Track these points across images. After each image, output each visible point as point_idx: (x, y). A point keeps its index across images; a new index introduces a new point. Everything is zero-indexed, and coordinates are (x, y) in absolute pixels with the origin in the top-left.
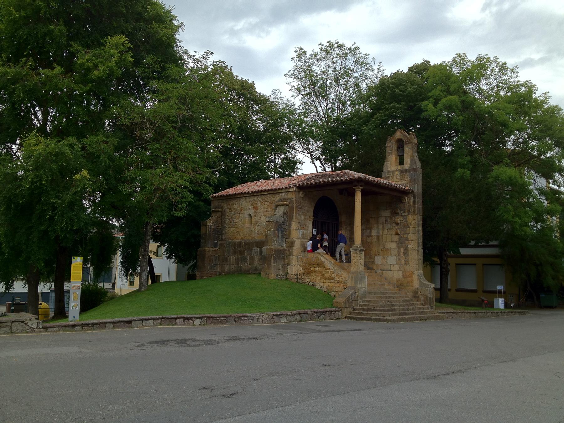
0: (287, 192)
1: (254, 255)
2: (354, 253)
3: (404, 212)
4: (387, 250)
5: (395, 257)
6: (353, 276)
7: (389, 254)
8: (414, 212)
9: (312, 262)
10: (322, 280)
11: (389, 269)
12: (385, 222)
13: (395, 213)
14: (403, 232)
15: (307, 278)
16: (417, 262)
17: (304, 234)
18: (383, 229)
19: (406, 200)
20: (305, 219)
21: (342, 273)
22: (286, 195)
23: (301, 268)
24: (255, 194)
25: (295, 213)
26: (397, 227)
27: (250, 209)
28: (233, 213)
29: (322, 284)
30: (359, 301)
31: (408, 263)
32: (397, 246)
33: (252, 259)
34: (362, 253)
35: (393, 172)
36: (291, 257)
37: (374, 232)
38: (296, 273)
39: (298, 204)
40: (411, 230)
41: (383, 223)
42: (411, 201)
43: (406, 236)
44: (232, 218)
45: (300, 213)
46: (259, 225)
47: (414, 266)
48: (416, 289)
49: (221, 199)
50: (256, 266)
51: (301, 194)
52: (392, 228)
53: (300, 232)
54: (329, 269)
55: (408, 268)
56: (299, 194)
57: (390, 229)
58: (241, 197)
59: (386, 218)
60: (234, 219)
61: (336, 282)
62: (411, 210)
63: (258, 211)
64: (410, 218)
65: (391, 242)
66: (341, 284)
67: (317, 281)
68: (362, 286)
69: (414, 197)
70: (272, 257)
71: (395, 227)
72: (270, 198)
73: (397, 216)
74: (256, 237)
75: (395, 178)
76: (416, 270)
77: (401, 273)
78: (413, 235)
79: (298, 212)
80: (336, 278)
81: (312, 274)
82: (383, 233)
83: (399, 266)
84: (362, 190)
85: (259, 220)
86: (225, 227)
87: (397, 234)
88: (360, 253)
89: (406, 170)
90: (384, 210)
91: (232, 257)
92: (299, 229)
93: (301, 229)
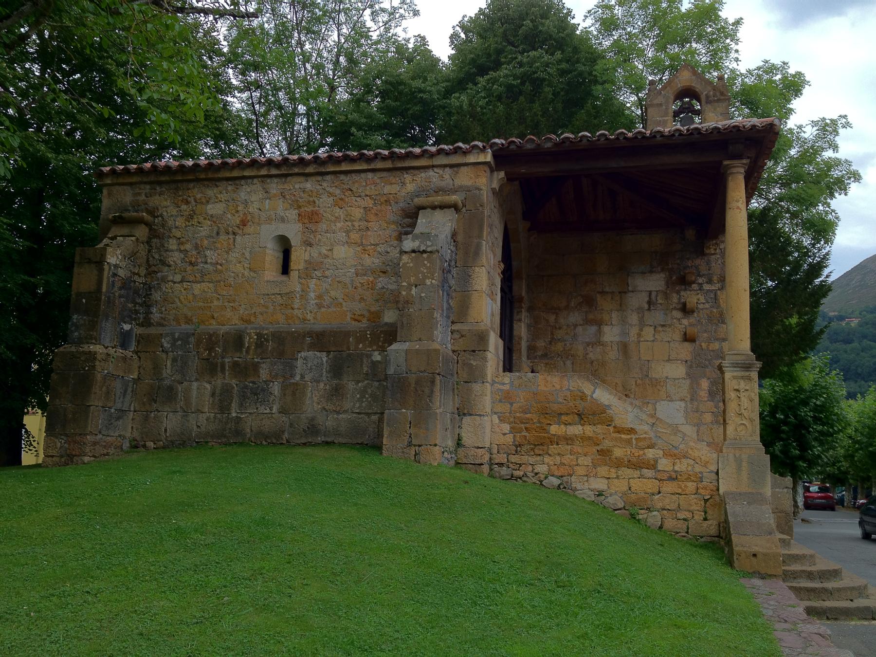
0: (451, 166)
1: (302, 377)
2: (734, 378)
3: (710, 282)
4: (656, 383)
5: (683, 404)
9: (555, 407)
10: (603, 470)
12: (646, 306)
15: (532, 460)
18: (642, 324)
22: (447, 176)
23: (506, 428)
24: (310, 169)
26: (685, 322)
27: (283, 220)
28: (205, 230)
32: (688, 374)
33: (294, 392)
36: (476, 387)
37: (611, 334)
41: (640, 310)
43: (716, 346)
44: (196, 247)
46: (327, 273)
49: (150, 183)
50: (313, 419)
52: (669, 322)
54: (632, 431)
57: (663, 326)
58: (244, 178)
60: (208, 253)
61: (665, 476)
63: (323, 226)
65: (669, 360)
66: (690, 484)
67: (581, 471)
70: (438, 382)
71: (679, 320)
72: (376, 184)
73: (685, 290)
74: (309, 317)
81: (553, 449)
82: (639, 335)
83: (695, 429)
85: (327, 256)
86: (164, 280)
87: (688, 338)
90: (643, 273)
91: (195, 385)
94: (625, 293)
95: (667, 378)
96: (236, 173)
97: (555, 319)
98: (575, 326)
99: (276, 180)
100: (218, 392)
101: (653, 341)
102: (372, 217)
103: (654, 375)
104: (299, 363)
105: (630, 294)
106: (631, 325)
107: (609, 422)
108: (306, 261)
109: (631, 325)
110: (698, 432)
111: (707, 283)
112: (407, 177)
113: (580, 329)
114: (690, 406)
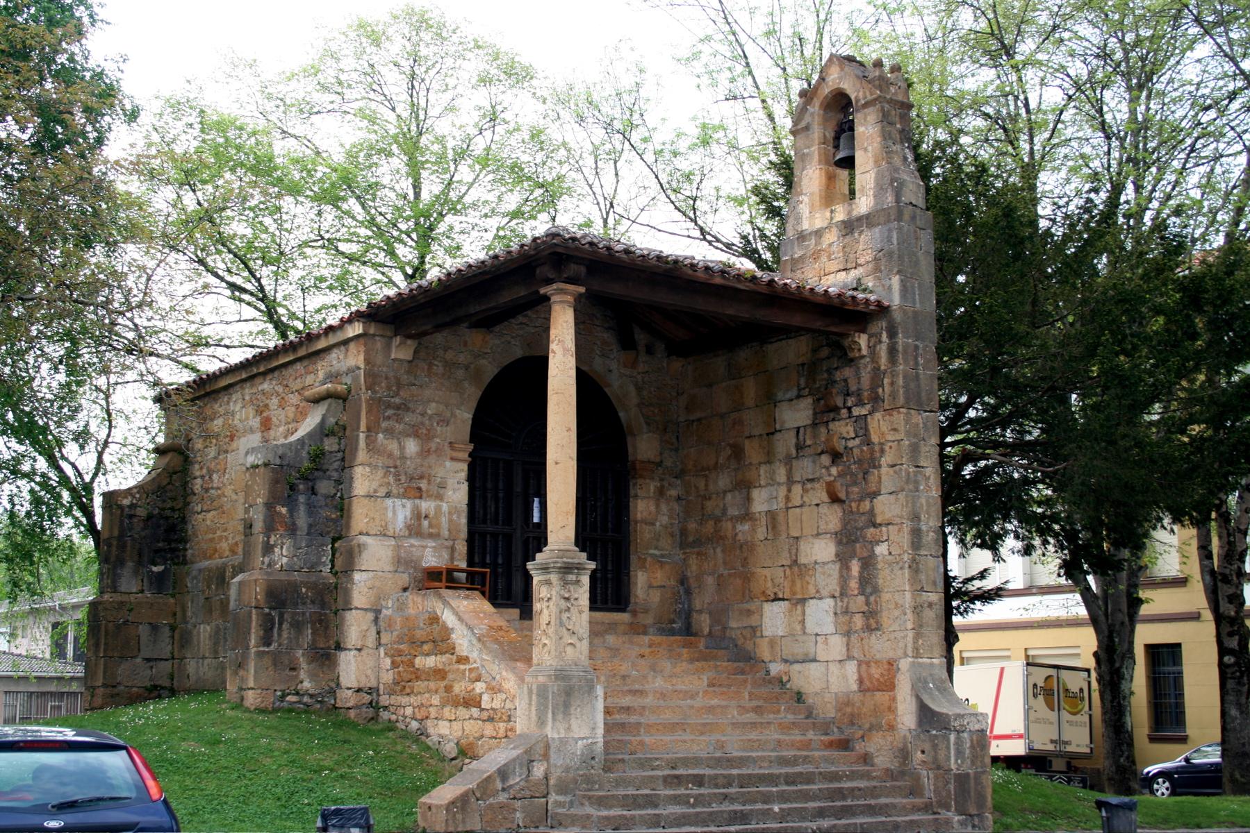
3: (860, 403)
5: (831, 602)
6: (534, 687)
7: (812, 591)
8: (893, 395)
10: (448, 712)
11: (811, 656)
12: (794, 452)
13: (826, 412)
14: (856, 489)
16: (910, 615)
17: (418, 516)
18: (790, 482)
19: (860, 350)
20: (425, 453)
21: (504, 673)
23: (388, 661)
25: (369, 429)
26: (834, 471)
28: (212, 452)
29: (443, 728)
30: (553, 797)
31: (877, 623)
32: (837, 555)
34: (578, 582)
35: (819, 233)
37: (761, 501)
38: (373, 684)
39: (381, 391)
40: (884, 478)
41: (788, 461)
42: (883, 350)
45: (399, 427)
47: (899, 635)
48: (905, 736)
51: (402, 351)
52: (817, 475)
53: (400, 512)
55: (880, 646)
56: (388, 347)
57: (812, 480)
59: (798, 432)
61: (485, 715)
62: (880, 390)
64: (879, 425)
65: (818, 534)
66: (501, 725)
68: (569, 729)
69: (892, 334)
70: (254, 617)
71: (827, 468)
73: (834, 420)
75: (824, 259)
76: (906, 655)
77: (851, 668)
78: (892, 497)
79: (384, 425)
80: (485, 697)
81: (420, 685)
82: (788, 499)
83: (845, 639)
84: (579, 299)
87: (835, 499)
88: (565, 583)
89: (867, 220)
92: (388, 495)
93: (404, 496)
94: (772, 434)
95: (816, 563)
97: (706, 485)
98: (725, 492)
99: (248, 384)
101: (801, 506)
103: (803, 560)
105: (778, 436)
106: (779, 484)
107: (452, 650)
109: (779, 484)
110: (848, 645)
111: (856, 405)
113: (729, 496)
114: (840, 604)
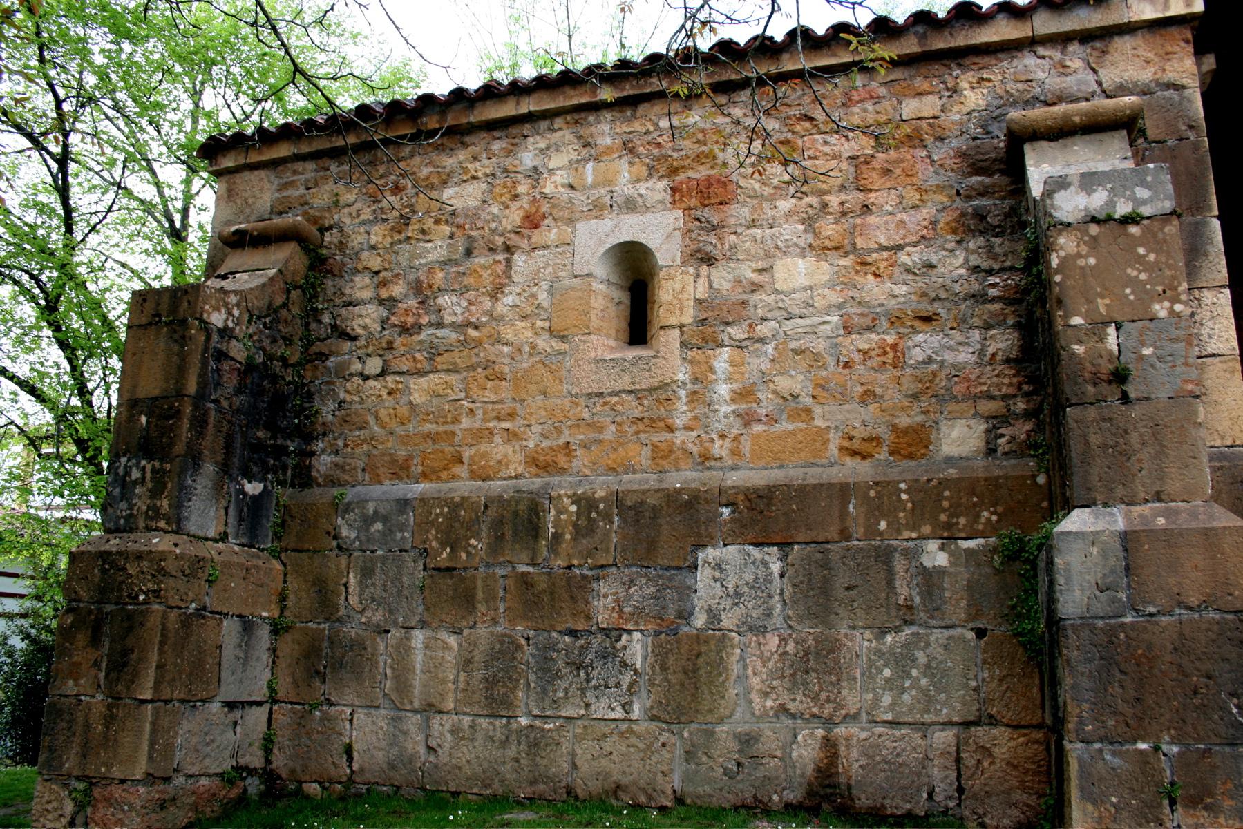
0: (1086, 37)
22: (1076, 63)
27: (630, 206)
28: (436, 249)
44: (417, 288)
46: (763, 330)
49: (315, 156)
50: (747, 741)
60: (445, 300)
63: (739, 212)
72: (877, 100)
74: (719, 448)
85: (756, 287)
86: (343, 374)
91: (419, 637)
96: (508, 109)
99: (608, 115)
100: (479, 656)
102: (874, 179)
104: (703, 576)
108: (699, 302)
112: (965, 80)
